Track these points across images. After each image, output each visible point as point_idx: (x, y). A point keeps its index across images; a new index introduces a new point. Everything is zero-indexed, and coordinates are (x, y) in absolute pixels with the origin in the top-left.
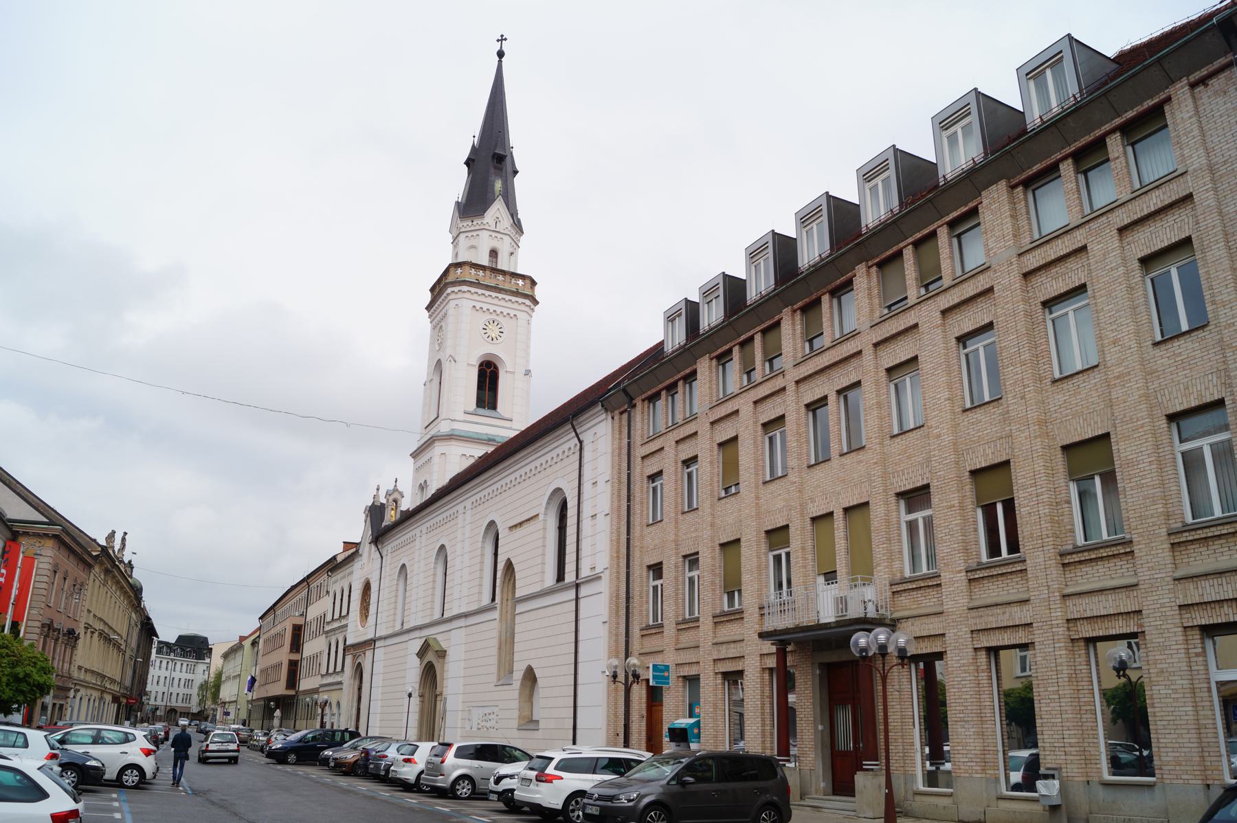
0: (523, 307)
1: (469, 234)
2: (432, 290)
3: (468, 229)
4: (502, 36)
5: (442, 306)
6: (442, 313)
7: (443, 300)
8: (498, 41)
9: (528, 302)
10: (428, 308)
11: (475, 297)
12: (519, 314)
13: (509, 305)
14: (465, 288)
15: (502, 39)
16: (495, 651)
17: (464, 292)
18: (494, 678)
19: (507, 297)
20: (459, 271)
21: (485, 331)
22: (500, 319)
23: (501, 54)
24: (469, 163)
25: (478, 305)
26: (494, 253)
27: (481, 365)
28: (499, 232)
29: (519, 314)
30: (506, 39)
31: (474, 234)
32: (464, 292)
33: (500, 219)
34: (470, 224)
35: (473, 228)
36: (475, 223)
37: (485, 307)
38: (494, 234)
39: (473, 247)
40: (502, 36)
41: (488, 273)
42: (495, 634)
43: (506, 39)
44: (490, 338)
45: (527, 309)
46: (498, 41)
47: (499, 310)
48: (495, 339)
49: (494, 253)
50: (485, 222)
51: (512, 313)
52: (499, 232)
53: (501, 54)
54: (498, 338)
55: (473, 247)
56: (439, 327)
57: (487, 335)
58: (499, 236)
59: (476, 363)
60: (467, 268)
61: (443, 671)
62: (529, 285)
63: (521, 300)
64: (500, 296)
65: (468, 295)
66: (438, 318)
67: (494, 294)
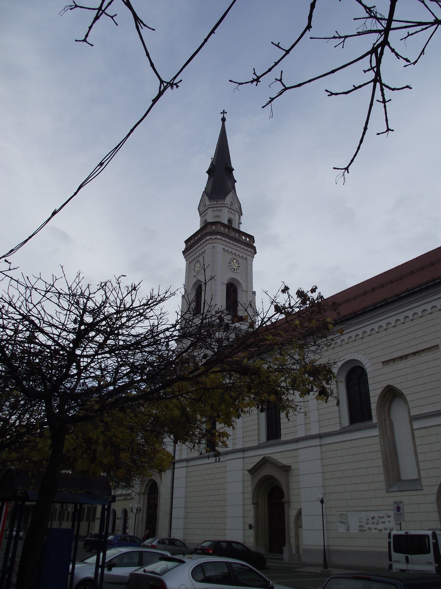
0: (249, 253)
1: (215, 209)
2: (186, 242)
3: (214, 206)
4: (224, 111)
5: (202, 246)
6: (203, 250)
7: (204, 242)
8: (221, 113)
9: (253, 251)
10: (184, 252)
11: (224, 243)
12: (248, 257)
13: (242, 251)
14: (219, 237)
15: (224, 112)
16: (380, 462)
17: (218, 239)
18: (383, 485)
19: (242, 246)
20: (214, 227)
21: (230, 265)
22: (237, 258)
23: (223, 120)
24: (208, 172)
25: (226, 249)
26: (230, 221)
27: (228, 285)
28: (233, 210)
29: (248, 257)
30: (226, 113)
31: (219, 209)
32: (218, 239)
33: (233, 203)
34: (216, 203)
35: (217, 206)
36: (219, 203)
37: (230, 250)
38: (230, 211)
39: (218, 216)
40: (224, 111)
41: (231, 230)
42: (378, 448)
43: (226, 113)
44: (233, 269)
45: (252, 255)
46: (221, 113)
47: (237, 253)
48: (235, 270)
49: (230, 221)
50: (226, 203)
51: (245, 256)
52: (233, 210)
53: (223, 120)
54: (237, 269)
55: (218, 216)
56: (196, 260)
57: (231, 267)
58: (233, 212)
59: (226, 282)
60: (220, 226)
61: (288, 483)
62: (252, 241)
63: (249, 249)
64: (239, 245)
65: (220, 241)
66: (193, 258)
67: (235, 243)
